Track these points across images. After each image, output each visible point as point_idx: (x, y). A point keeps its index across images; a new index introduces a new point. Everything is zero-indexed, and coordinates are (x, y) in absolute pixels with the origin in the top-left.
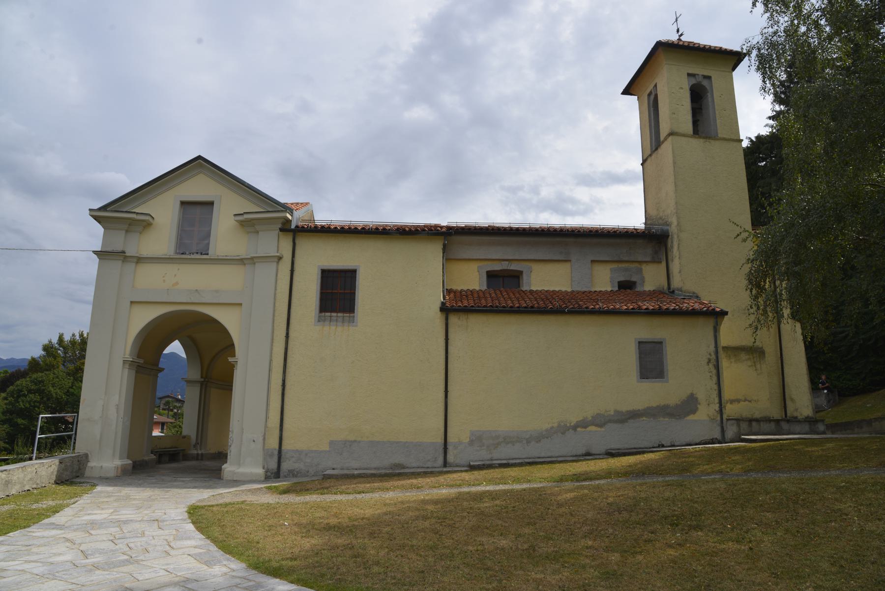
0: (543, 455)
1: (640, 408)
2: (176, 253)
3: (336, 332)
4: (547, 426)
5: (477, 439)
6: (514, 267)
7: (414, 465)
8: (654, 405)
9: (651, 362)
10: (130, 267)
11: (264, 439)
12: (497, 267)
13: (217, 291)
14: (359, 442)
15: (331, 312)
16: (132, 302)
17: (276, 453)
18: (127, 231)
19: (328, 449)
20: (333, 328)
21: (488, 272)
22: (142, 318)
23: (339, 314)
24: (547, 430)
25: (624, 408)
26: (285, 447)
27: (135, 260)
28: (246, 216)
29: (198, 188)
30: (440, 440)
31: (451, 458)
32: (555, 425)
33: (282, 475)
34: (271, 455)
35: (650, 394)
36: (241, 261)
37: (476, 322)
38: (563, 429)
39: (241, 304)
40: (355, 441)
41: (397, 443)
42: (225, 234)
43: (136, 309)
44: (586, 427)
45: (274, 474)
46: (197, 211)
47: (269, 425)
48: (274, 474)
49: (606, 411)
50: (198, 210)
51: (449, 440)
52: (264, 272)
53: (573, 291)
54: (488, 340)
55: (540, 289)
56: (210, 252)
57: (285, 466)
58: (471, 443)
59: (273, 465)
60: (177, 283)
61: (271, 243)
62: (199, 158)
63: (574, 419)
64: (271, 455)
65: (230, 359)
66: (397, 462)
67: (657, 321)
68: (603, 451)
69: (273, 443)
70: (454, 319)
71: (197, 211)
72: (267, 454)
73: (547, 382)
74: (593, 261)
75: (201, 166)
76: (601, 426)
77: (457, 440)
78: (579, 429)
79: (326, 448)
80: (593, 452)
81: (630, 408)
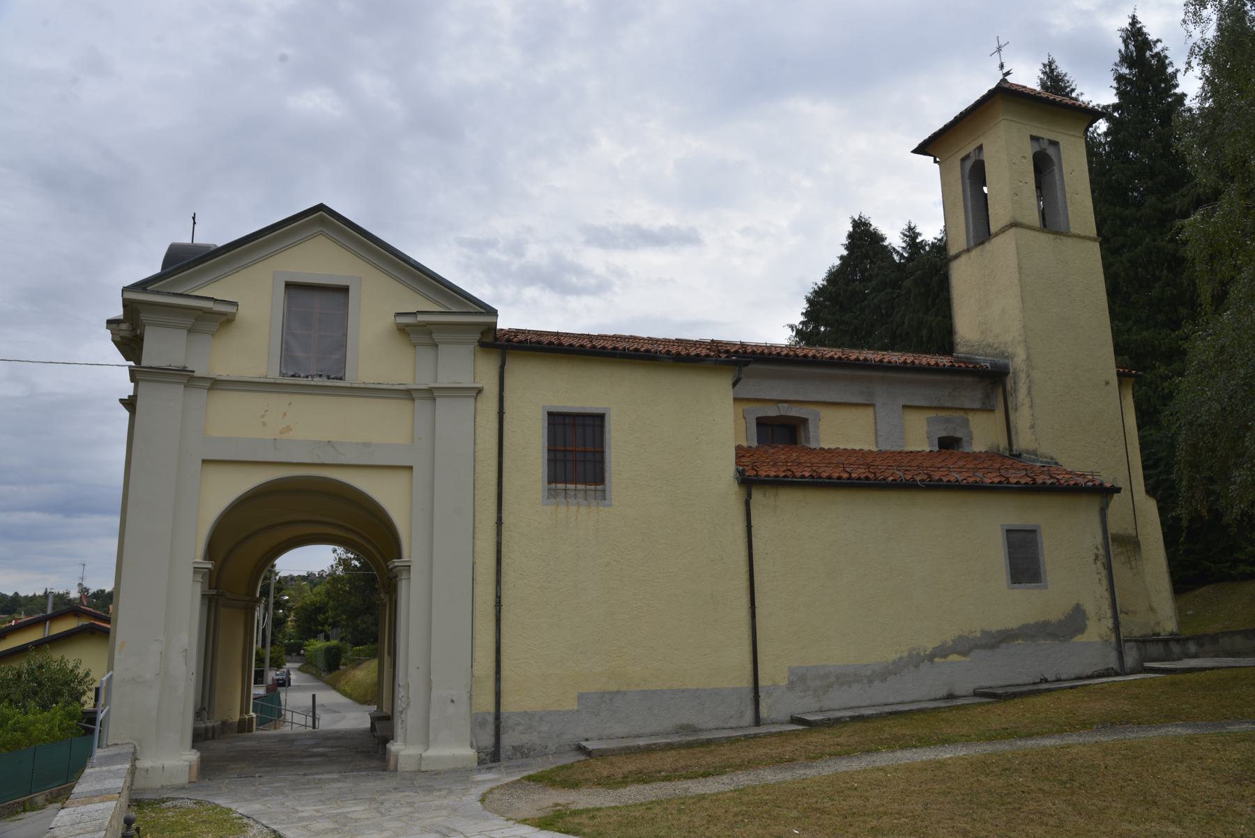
0: (891, 700)
1: (1014, 626)
2: (283, 375)
3: (578, 515)
4: (893, 657)
5: (799, 680)
6: (795, 412)
7: (711, 725)
8: (1032, 622)
9: (1024, 561)
10: (198, 397)
11: (471, 698)
12: (771, 411)
13: (366, 445)
14: (625, 693)
15: (576, 483)
16: (204, 461)
17: (491, 719)
18: (189, 331)
19: (576, 708)
20: (573, 509)
21: (758, 419)
22: (225, 490)
23: (580, 487)
24: (894, 663)
25: (995, 627)
26: (508, 706)
27: (208, 385)
28: (421, 318)
29: (318, 261)
30: (746, 683)
31: (764, 712)
32: (905, 654)
33: (502, 755)
34: (482, 724)
35: (1021, 606)
36: (408, 394)
37: (788, 500)
38: (917, 660)
39: (411, 468)
40: (618, 692)
41: (683, 691)
42: (372, 346)
43: (215, 474)
44: (945, 656)
45: (492, 756)
46: (315, 302)
47: (476, 673)
48: (492, 756)
49: (971, 632)
50: (316, 301)
51: (761, 683)
52: (451, 414)
53: (880, 452)
54: (803, 528)
55: (833, 446)
56: (349, 374)
57: (508, 740)
58: (791, 686)
59: (487, 740)
60: (288, 429)
61: (462, 366)
62: (321, 207)
63: (929, 645)
64: (482, 724)
65: (397, 562)
66: (685, 722)
67: (1029, 500)
68: (971, 691)
69: (486, 703)
70: (757, 496)
71: (315, 302)
72: (477, 722)
73: (886, 590)
74: (904, 407)
75: (322, 221)
76: (965, 654)
77: (770, 683)
78: (936, 660)
79: (571, 705)
80: (958, 693)
81: (1001, 627)
